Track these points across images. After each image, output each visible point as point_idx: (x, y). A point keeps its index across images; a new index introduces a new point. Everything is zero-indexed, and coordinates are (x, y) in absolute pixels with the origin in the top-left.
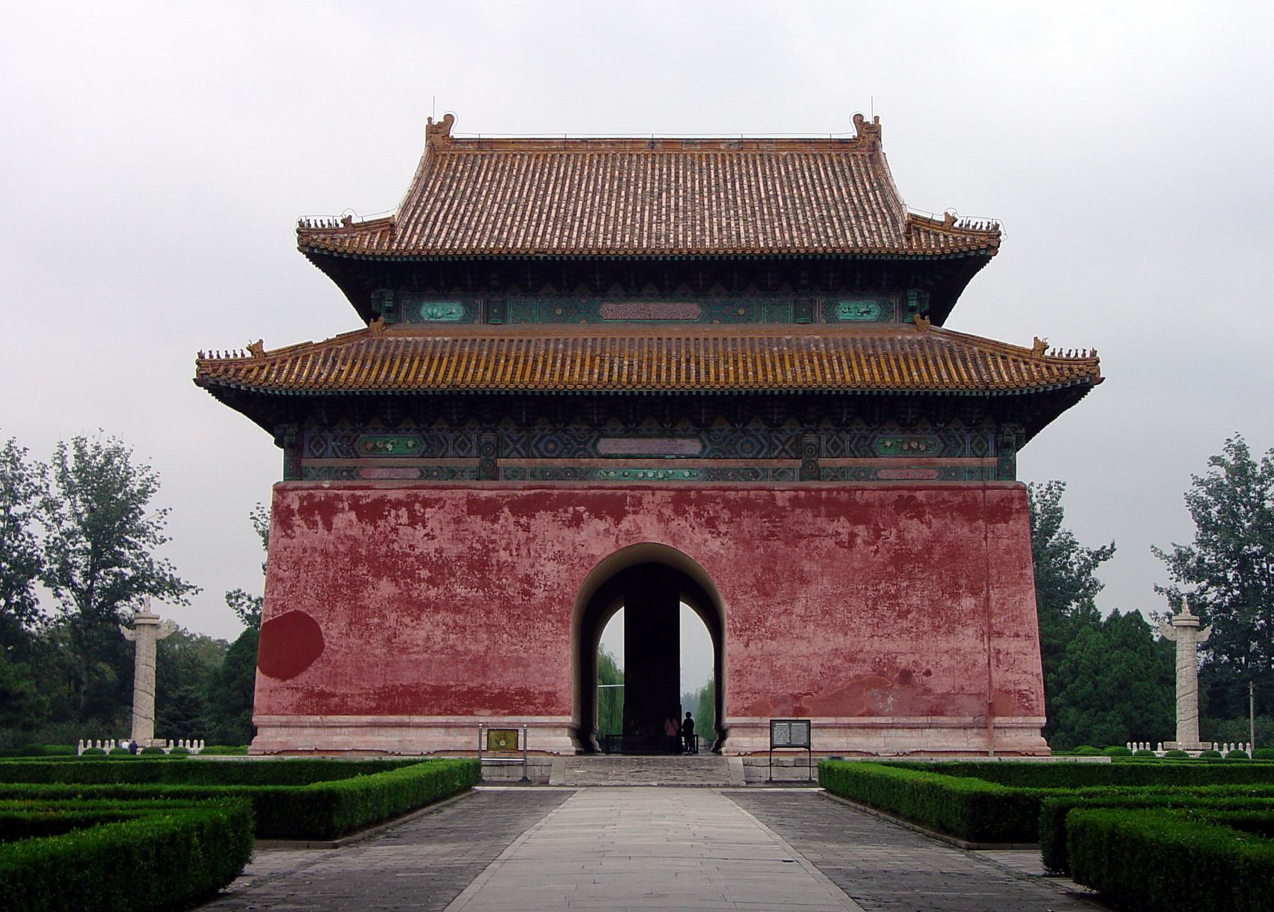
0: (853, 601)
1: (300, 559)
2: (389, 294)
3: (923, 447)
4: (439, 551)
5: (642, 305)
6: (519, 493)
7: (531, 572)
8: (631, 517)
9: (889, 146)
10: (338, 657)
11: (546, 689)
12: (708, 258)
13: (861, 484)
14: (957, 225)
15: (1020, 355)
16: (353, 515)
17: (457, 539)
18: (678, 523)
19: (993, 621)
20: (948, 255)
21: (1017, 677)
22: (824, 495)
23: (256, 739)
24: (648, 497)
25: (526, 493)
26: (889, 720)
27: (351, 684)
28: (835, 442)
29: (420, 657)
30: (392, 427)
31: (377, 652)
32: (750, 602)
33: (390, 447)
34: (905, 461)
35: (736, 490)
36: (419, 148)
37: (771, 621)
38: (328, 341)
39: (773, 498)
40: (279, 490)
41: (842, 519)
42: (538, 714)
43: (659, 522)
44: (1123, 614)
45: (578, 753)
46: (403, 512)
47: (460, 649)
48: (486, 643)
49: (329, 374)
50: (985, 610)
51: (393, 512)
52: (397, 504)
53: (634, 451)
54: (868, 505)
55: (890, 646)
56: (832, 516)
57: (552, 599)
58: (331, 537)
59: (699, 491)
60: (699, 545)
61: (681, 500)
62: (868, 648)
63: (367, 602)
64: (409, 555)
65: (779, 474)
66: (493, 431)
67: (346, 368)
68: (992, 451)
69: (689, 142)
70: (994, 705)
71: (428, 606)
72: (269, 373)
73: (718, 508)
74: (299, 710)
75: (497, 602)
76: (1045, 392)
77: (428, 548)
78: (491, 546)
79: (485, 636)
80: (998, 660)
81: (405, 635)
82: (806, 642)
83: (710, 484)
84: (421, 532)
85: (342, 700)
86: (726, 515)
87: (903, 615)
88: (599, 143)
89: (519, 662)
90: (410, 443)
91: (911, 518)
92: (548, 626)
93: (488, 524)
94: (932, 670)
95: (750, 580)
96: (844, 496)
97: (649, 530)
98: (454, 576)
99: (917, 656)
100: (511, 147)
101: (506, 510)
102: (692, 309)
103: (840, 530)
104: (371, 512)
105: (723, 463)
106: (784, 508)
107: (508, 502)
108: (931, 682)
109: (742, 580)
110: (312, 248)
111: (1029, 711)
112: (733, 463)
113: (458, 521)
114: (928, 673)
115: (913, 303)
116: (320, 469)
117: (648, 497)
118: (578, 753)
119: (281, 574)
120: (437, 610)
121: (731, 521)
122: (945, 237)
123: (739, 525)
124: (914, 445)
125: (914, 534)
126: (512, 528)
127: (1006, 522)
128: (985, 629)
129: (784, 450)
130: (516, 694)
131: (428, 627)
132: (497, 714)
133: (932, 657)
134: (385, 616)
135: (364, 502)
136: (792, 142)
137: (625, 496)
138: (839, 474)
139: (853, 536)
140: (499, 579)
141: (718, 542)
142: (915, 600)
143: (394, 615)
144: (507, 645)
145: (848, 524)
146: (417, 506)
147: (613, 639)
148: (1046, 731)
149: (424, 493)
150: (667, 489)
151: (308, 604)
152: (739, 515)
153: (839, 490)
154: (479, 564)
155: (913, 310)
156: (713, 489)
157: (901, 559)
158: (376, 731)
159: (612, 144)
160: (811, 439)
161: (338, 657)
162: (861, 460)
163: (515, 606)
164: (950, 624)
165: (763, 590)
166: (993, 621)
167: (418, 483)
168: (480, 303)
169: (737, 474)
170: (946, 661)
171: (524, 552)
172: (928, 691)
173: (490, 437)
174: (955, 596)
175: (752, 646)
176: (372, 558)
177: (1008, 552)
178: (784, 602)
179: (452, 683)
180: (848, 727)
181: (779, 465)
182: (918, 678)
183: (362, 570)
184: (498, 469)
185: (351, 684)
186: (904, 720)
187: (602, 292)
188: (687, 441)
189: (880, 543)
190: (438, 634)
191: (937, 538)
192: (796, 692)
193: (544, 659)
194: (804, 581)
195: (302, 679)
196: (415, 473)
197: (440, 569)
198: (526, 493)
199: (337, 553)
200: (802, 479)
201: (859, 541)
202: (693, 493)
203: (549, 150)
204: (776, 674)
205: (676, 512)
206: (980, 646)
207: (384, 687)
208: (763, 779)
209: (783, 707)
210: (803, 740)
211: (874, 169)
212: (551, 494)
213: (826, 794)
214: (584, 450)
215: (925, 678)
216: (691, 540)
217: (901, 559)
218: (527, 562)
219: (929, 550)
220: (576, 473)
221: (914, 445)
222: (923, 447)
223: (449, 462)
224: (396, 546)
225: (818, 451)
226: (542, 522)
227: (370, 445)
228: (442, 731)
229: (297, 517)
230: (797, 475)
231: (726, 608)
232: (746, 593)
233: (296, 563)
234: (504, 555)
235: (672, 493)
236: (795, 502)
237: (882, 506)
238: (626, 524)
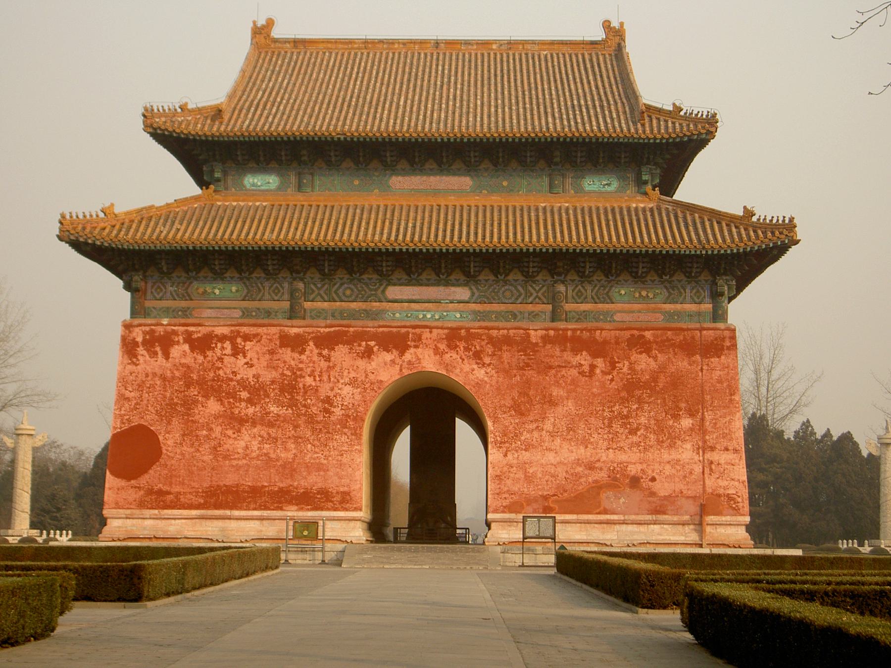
0: (592, 420)
1: (143, 382)
3: (651, 295)
4: (257, 376)
5: (425, 178)
6: (322, 330)
7: (331, 394)
8: (412, 350)
9: (631, 48)
10: (173, 462)
11: (342, 489)
12: (478, 140)
13: (600, 324)
14: (682, 113)
15: (731, 220)
16: (186, 347)
17: (271, 367)
18: (451, 356)
19: (707, 437)
20: (674, 138)
21: (726, 483)
22: (569, 333)
23: (106, 529)
24: (426, 334)
25: (327, 330)
26: (621, 517)
27: (183, 484)
28: (579, 291)
29: (240, 463)
30: (219, 276)
31: (205, 458)
32: (509, 421)
33: (217, 291)
34: (636, 306)
35: (499, 329)
36: (243, 45)
37: (525, 436)
38: (168, 204)
39: (528, 335)
40: (127, 326)
41: (584, 353)
42: (336, 509)
43: (435, 354)
44: (835, 436)
46: (227, 345)
47: (273, 456)
48: (294, 451)
49: (169, 233)
50: (701, 429)
51: (219, 345)
52: (222, 338)
54: (606, 342)
55: (622, 457)
56: (576, 351)
57: (348, 416)
58: (169, 365)
59: (468, 330)
60: (469, 374)
61: (453, 337)
62: (604, 458)
63: (197, 417)
64: (231, 380)
65: (533, 316)
66: (302, 280)
67: (183, 228)
68: (707, 299)
69: (467, 43)
70: (707, 507)
71: (247, 421)
72: (120, 230)
73: (483, 343)
74: (142, 505)
75: (303, 418)
76: (751, 251)
77: (249, 374)
78: (298, 373)
79: (293, 446)
80: (711, 469)
81: (229, 444)
82: (555, 453)
83: (477, 324)
84: (241, 361)
85: (176, 497)
86: (489, 349)
87: (633, 432)
88: (393, 43)
89: (320, 468)
90: (234, 289)
91: (641, 353)
92: (344, 438)
93: (296, 355)
94: (657, 477)
95: (508, 402)
96: (586, 335)
97: (427, 361)
98: (268, 397)
99: (645, 466)
100: (321, 46)
101: (311, 343)
102: (465, 182)
103: (583, 362)
104: (201, 345)
105: (488, 307)
106: (537, 344)
107: (312, 338)
108: (656, 486)
109: (503, 402)
110: (155, 129)
111: (737, 511)
112: (496, 307)
113: (272, 352)
114: (653, 479)
116: (161, 309)
117: (426, 334)
119: (127, 394)
120: (254, 424)
121: (493, 355)
122: (673, 123)
123: (500, 357)
125: (643, 366)
126: (315, 358)
127: (719, 357)
128: (700, 444)
129: (537, 296)
130: (318, 493)
131: (247, 438)
132: (301, 509)
133: (657, 466)
134: (211, 429)
135: (195, 336)
136: (552, 43)
137: (408, 333)
138: (582, 316)
139: (593, 367)
140: (305, 400)
141: (483, 371)
142: (643, 420)
143: (219, 429)
144: (311, 454)
145: (588, 358)
146: (239, 340)
148: (749, 528)
149: (245, 330)
150: (442, 328)
151: (149, 419)
152: (501, 350)
153: (582, 330)
154: (289, 388)
156: (480, 328)
157: (632, 388)
158: (204, 522)
159: (404, 44)
160: (561, 288)
161: (173, 462)
162: (600, 306)
163: (318, 422)
164: (672, 440)
165: (519, 410)
166: (707, 437)
167: (241, 321)
169: (499, 316)
170: (668, 470)
171: (325, 378)
172: (653, 494)
174: (676, 417)
175: (510, 456)
176: (201, 383)
177: (720, 381)
178: (536, 421)
179: (266, 484)
180: (588, 522)
181: (533, 309)
182: (645, 483)
183: (193, 391)
185: (183, 484)
186: (633, 517)
187: (390, 168)
189: (615, 373)
190: (255, 445)
191: (662, 369)
192: (545, 493)
193: (341, 465)
194: (552, 403)
195: (144, 480)
196: (237, 314)
197: (257, 392)
198: (327, 330)
199: (173, 378)
201: (598, 371)
202: (463, 331)
203: (352, 48)
204: (529, 479)
205: (449, 346)
206: (696, 458)
207: (211, 487)
208: (517, 565)
209: (535, 506)
210: (549, 533)
211: (618, 66)
212: (348, 331)
213: (559, 575)
214: (375, 295)
215: (650, 483)
216: (461, 370)
217: (632, 388)
218: (327, 386)
219: (655, 379)
221: (644, 293)
222: (651, 295)
223: (266, 304)
224: (221, 372)
226: (341, 354)
227: (201, 290)
228: (257, 522)
229: (141, 348)
230: (548, 315)
231: (490, 424)
232: (505, 413)
233: (139, 386)
234: (309, 381)
235: (446, 331)
236: (546, 339)
237: (617, 343)
238: (408, 356)
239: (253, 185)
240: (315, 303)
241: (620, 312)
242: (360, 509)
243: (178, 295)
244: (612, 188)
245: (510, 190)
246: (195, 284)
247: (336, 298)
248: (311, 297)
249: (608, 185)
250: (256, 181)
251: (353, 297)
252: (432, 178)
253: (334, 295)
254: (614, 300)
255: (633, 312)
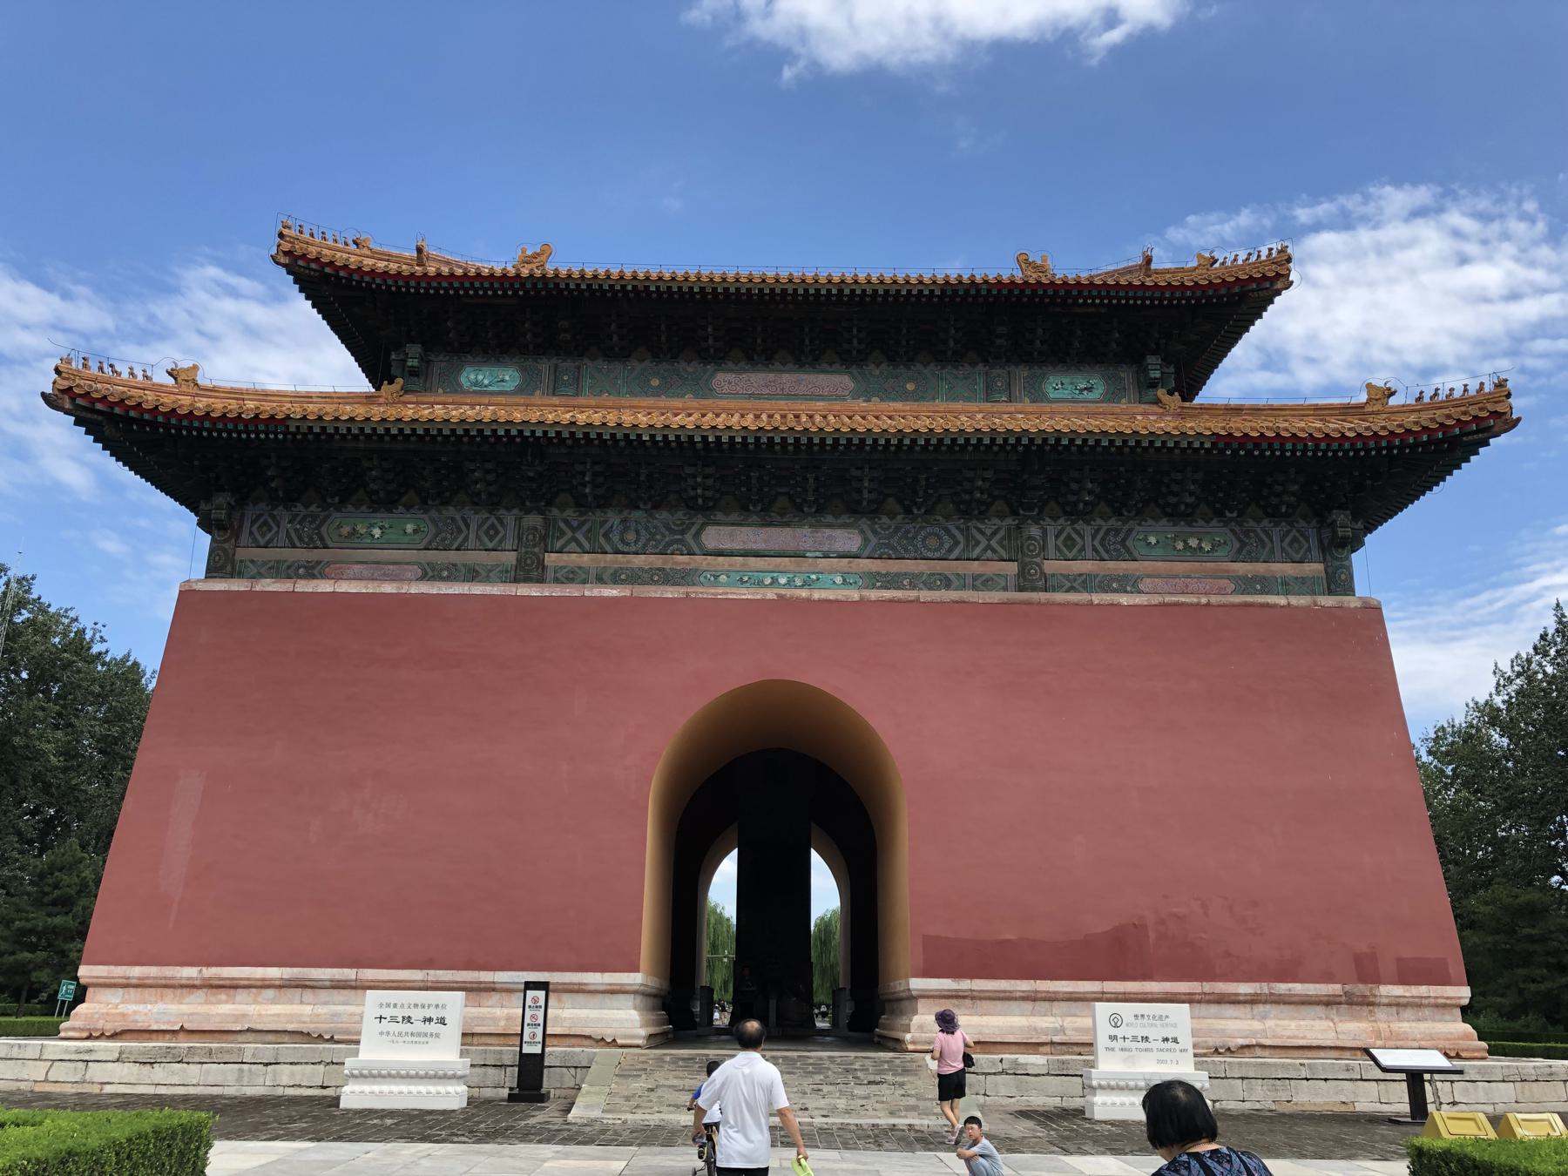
2: (414, 350)
3: (1207, 547)
5: (771, 376)
28: (1069, 537)
30: (386, 502)
33: (377, 532)
34: (1180, 567)
45: (659, 1040)
53: (760, 546)
66: (541, 512)
68: (1315, 553)
90: (410, 528)
105: (894, 566)
112: (910, 566)
115: (1157, 374)
116: (264, 564)
118: (659, 1040)
124: (1193, 542)
147: (723, 887)
148: (1468, 1012)
155: (1153, 385)
160: (1035, 531)
162: (1111, 564)
168: (545, 366)
173: (534, 520)
184: (544, 568)
188: (838, 532)
200: (1021, 589)
214: (682, 542)
220: (667, 578)
221: (1193, 542)
222: (1207, 547)
225: (1044, 548)
227: (345, 530)
230: (1012, 582)
239: (476, 383)
240: (565, 557)
241: (1149, 576)
242: (637, 970)
243: (300, 539)
244: (1095, 395)
245: (916, 397)
246: (337, 517)
247: (608, 548)
248: (558, 545)
249: (1089, 389)
250: (480, 377)
251: (640, 544)
252: (786, 377)
253: (602, 540)
254: (1136, 555)
255: (1175, 576)
